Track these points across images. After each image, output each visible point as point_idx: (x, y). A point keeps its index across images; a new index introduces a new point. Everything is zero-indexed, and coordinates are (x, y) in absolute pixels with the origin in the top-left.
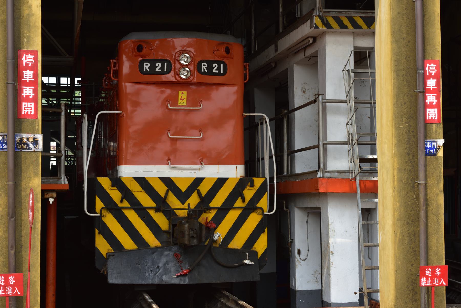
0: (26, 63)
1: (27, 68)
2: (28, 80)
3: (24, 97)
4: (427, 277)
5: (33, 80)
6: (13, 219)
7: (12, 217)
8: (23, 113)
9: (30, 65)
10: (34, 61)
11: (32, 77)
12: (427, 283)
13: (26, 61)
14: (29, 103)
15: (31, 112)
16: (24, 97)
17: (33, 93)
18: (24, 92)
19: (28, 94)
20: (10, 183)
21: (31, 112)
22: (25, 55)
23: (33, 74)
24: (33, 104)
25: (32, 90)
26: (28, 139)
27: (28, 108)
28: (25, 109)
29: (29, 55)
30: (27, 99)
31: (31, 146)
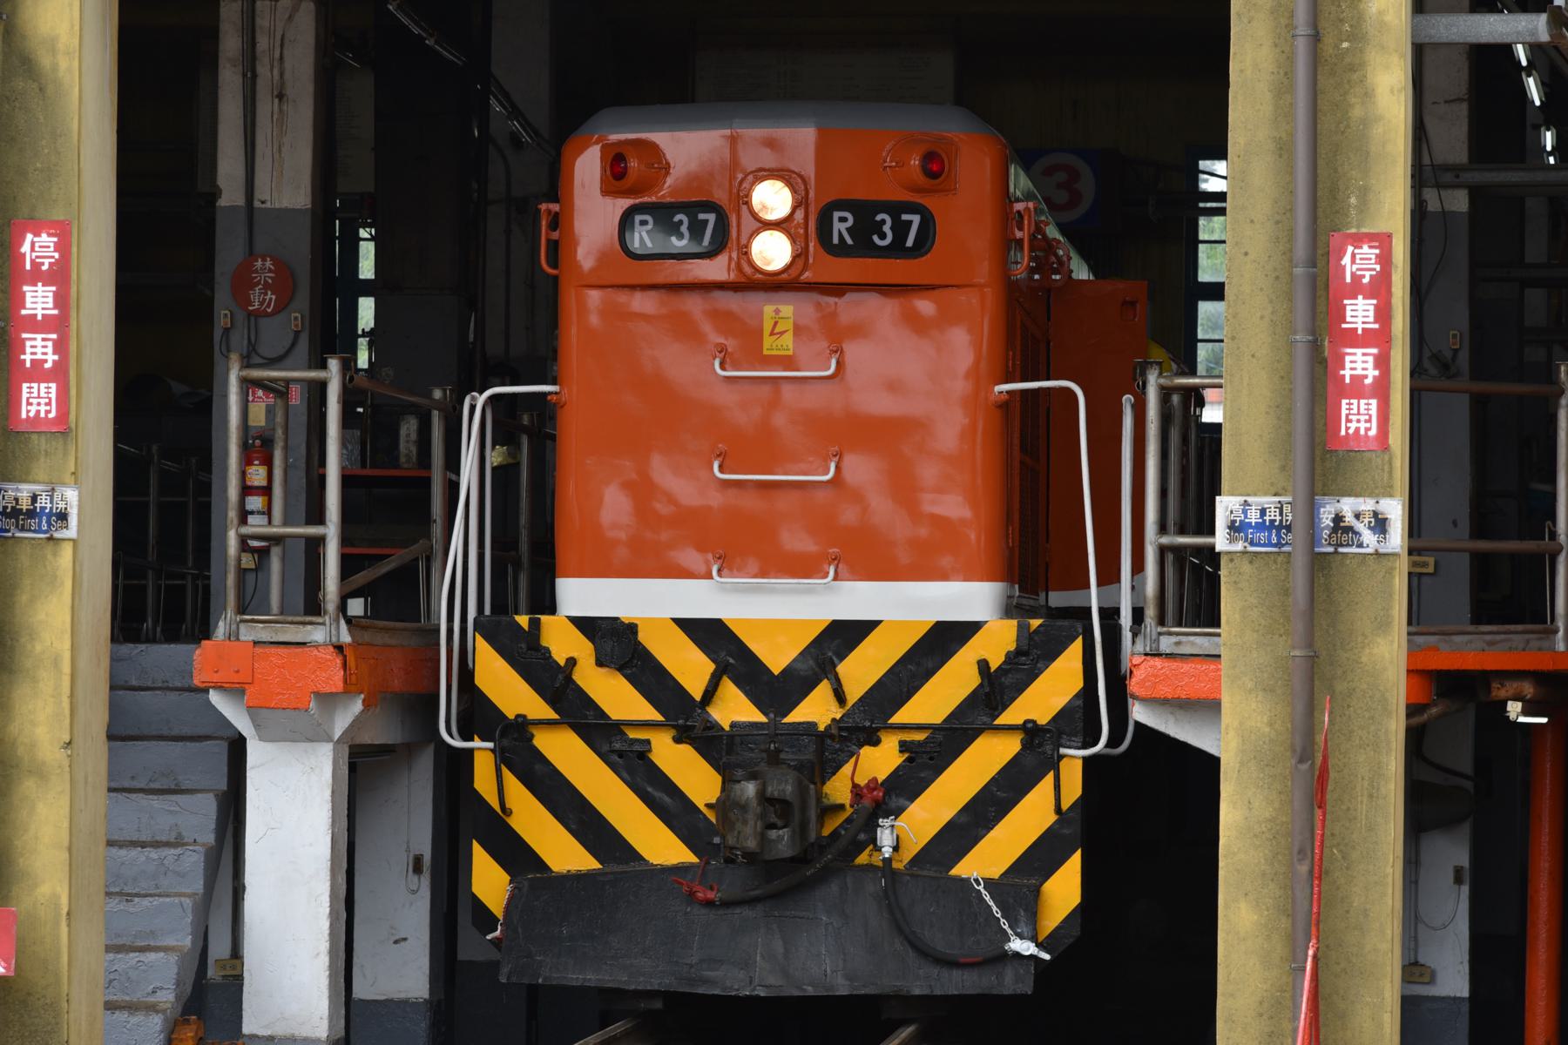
0: (1353, 274)
1: (1356, 289)
2: (1360, 327)
3: (1348, 380)
7: (1301, 761)
8: (1343, 432)
10: (1378, 268)
13: (1355, 267)
15: (1367, 429)
16: (1348, 380)
17: (1376, 367)
18: (1348, 365)
20: (1297, 653)
21: (1367, 429)
22: (1350, 249)
23: (1377, 307)
24: (1374, 402)
25: (1370, 359)
26: (1357, 516)
27: (1358, 418)
28: (1348, 421)
29: (1365, 249)
30: (1357, 389)
31: (1369, 538)
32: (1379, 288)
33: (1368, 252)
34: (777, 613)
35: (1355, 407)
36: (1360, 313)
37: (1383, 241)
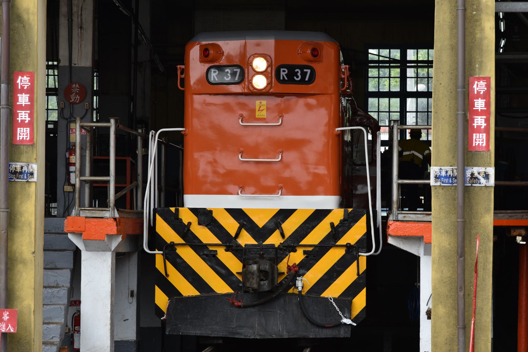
0: (477, 91)
1: (478, 96)
2: (480, 109)
3: (475, 127)
6: (462, 259)
7: (461, 257)
8: (474, 145)
9: (482, 93)
10: (486, 89)
11: (484, 106)
13: (478, 89)
15: (482, 144)
16: (475, 127)
17: (485, 123)
18: (476, 122)
19: (479, 124)
20: (459, 220)
21: (482, 144)
22: (476, 82)
23: (485, 102)
24: (485, 135)
25: (483, 120)
26: (479, 173)
27: (479, 140)
28: (476, 141)
29: (481, 82)
30: (479, 130)
31: (483, 181)
32: (486, 96)
33: (482, 83)
35: (478, 136)
36: (480, 104)
37: (487, 80)
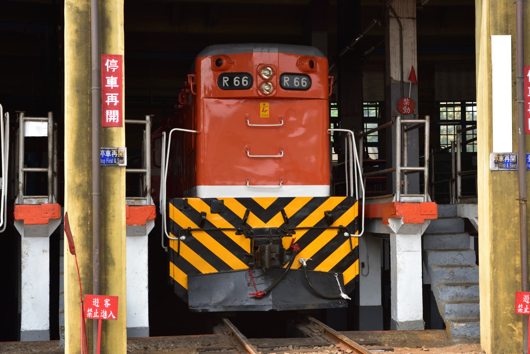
0: (109, 69)
1: (111, 73)
3: (108, 104)
4: (94, 308)
5: (117, 86)
9: (114, 71)
11: (116, 84)
12: (93, 315)
14: (114, 111)
18: (108, 99)
19: (112, 101)
21: (115, 120)
22: (108, 60)
24: (117, 111)
25: (116, 97)
28: (109, 117)
29: (113, 60)
30: (112, 107)
34: (265, 194)
35: (111, 113)
36: (112, 82)
37: (117, 57)
